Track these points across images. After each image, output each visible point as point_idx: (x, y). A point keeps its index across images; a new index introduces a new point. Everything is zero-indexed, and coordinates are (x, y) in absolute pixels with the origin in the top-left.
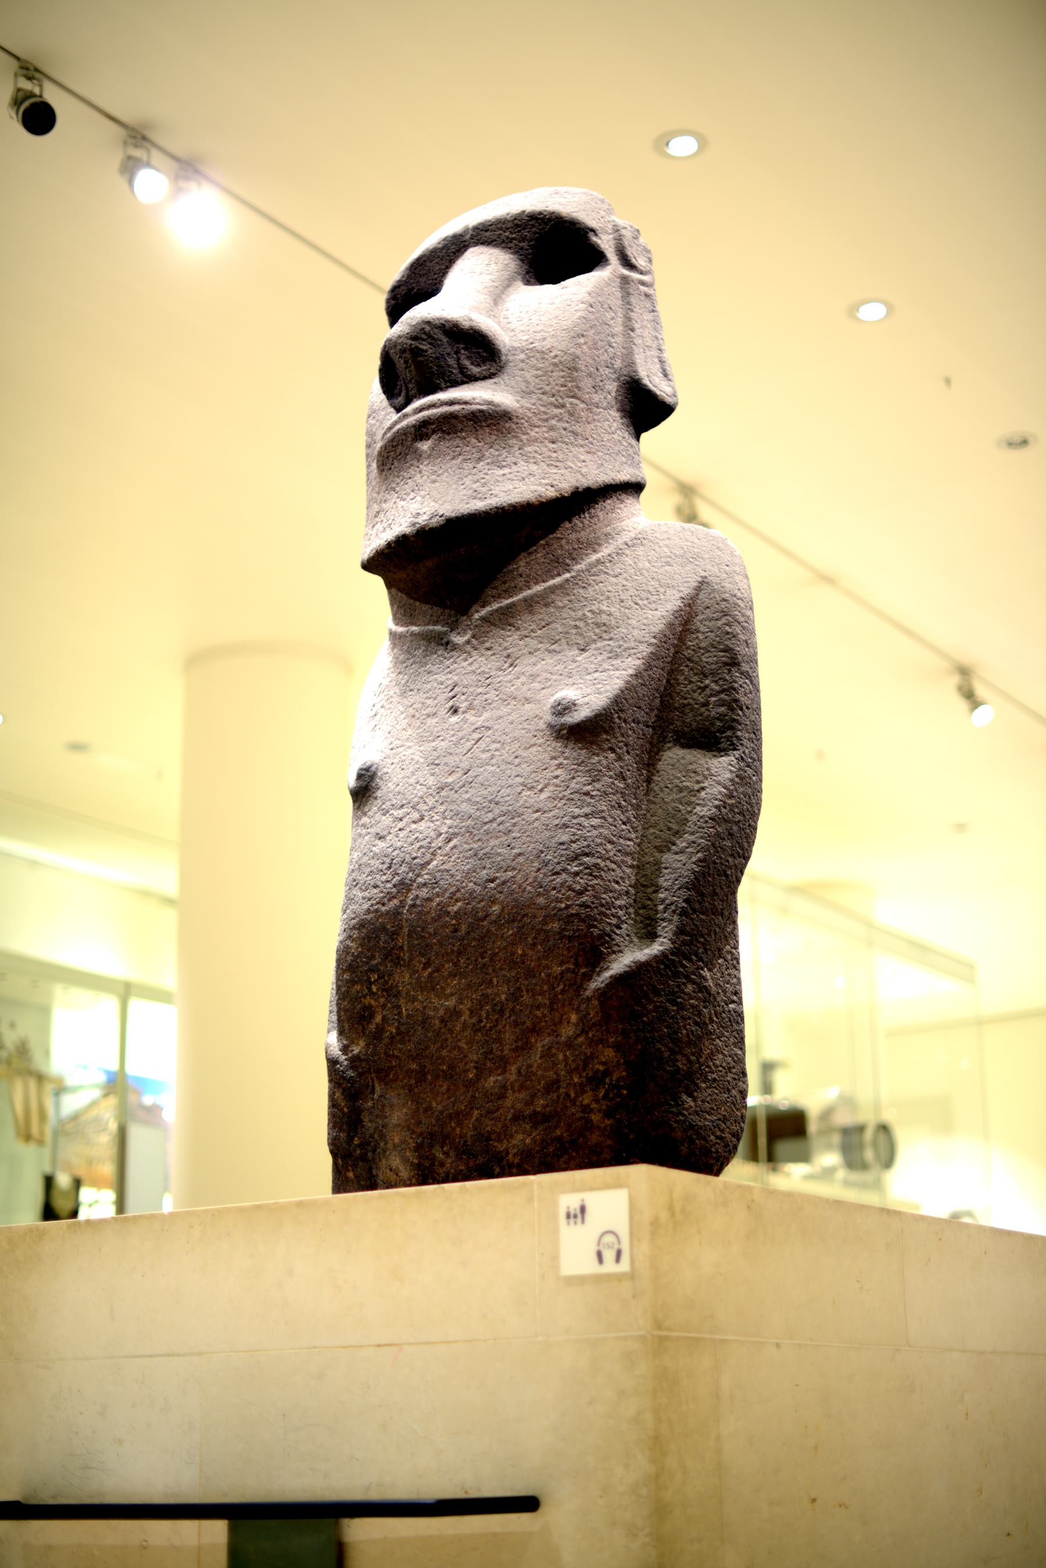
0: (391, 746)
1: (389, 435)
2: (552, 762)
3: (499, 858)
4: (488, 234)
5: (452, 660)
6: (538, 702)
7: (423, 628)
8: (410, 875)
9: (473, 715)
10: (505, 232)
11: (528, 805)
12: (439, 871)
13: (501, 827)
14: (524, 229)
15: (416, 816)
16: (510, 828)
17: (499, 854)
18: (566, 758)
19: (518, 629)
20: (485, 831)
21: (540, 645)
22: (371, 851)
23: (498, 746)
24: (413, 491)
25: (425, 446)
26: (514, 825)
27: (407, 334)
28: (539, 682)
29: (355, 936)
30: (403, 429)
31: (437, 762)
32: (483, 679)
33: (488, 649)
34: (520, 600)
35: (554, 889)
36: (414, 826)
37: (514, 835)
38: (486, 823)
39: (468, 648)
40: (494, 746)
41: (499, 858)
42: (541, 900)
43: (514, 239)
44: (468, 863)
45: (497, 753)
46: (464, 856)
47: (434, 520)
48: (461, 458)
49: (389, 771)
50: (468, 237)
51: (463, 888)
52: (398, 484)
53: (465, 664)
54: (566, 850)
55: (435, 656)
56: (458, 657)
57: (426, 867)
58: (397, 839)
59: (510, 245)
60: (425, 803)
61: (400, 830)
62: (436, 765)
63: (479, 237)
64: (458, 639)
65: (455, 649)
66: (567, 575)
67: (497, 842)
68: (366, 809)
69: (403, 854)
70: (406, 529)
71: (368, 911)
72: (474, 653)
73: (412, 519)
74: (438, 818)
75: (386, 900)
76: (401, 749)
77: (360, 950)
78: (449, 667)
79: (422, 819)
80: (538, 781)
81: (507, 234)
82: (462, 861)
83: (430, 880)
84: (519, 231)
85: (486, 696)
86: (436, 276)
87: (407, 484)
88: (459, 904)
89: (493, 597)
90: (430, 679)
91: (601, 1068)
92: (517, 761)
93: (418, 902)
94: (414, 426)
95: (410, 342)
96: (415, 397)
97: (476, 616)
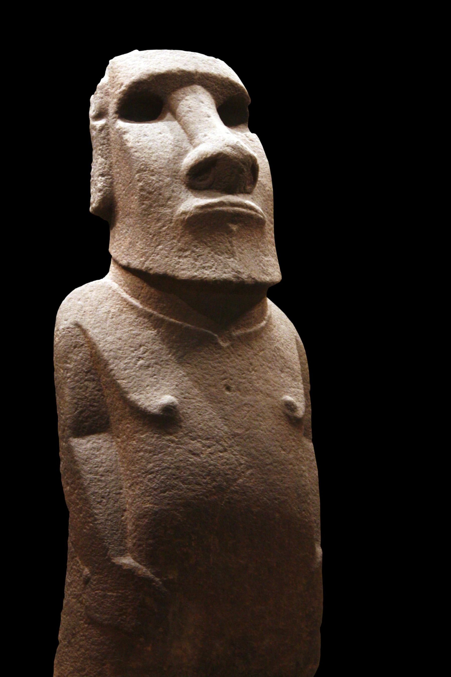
0: (183, 396)
1: (209, 210)
2: (290, 437)
3: (279, 487)
4: (207, 81)
5: (218, 355)
6: (273, 397)
7: (197, 328)
8: (225, 483)
9: (241, 395)
10: (216, 85)
11: (286, 459)
12: (246, 486)
13: (275, 469)
14: (225, 88)
15: (221, 448)
16: (281, 471)
17: (278, 485)
18: (295, 436)
19: (252, 348)
20: (268, 469)
21: (264, 362)
22: (188, 461)
23: (261, 419)
24: (227, 253)
25: (234, 228)
26: (282, 469)
27: (242, 159)
28: (271, 385)
29: (181, 510)
30: (223, 212)
31: (226, 417)
32: (240, 374)
33: (240, 356)
34: (253, 332)
35: (304, 511)
36: (221, 454)
37: (283, 475)
38: (267, 465)
39: (228, 351)
40: (259, 418)
41: (279, 487)
42: (298, 515)
43: (218, 91)
44: (262, 486)
45: (261, 423)
46: (259, 481)
47: (250, 280)
48: (251, 243)
49: (189, 412)
50: (196, 77)
51: (261, 499)
52: (209, 241)
53: (227, 360)
54: (305, 489)
55: (207, 349)
56: (223, 355)
57: (235, 482)
58: (209, 459)
59: (215, 93)
60: (225, 441)
61: (210, 453)
62: (225, 419)
63: (203, 81)
64: (224, 345)
65: (221, 349)
66: (265, 322)
67: (275, 477)
68: (171, 430)
69: (218, 470)
70: (233, 278)
71: (194, 498)
72: (232, 355)
73: (234, 273)
74: (237, 453)
75: (208, 494)
76: (194, 401)
77: (185, 519)
78: (217, 359)
79: (225, 450)
80: (286, 446)
81: (216, 87)
82: (258, 484)
83: (240, 490)
84: (222, 88)
85: (245, 385)
86: (168, 89)
87: (219, 245)
88: (259, 508)
89: (242, 325)
90: (205, 362)
91: (312, 609)
92: (273, 431)
93: (232, 501)
94: (231, 214)
95: (241, 164)
96: (216, 189)
97: (234, 334)
